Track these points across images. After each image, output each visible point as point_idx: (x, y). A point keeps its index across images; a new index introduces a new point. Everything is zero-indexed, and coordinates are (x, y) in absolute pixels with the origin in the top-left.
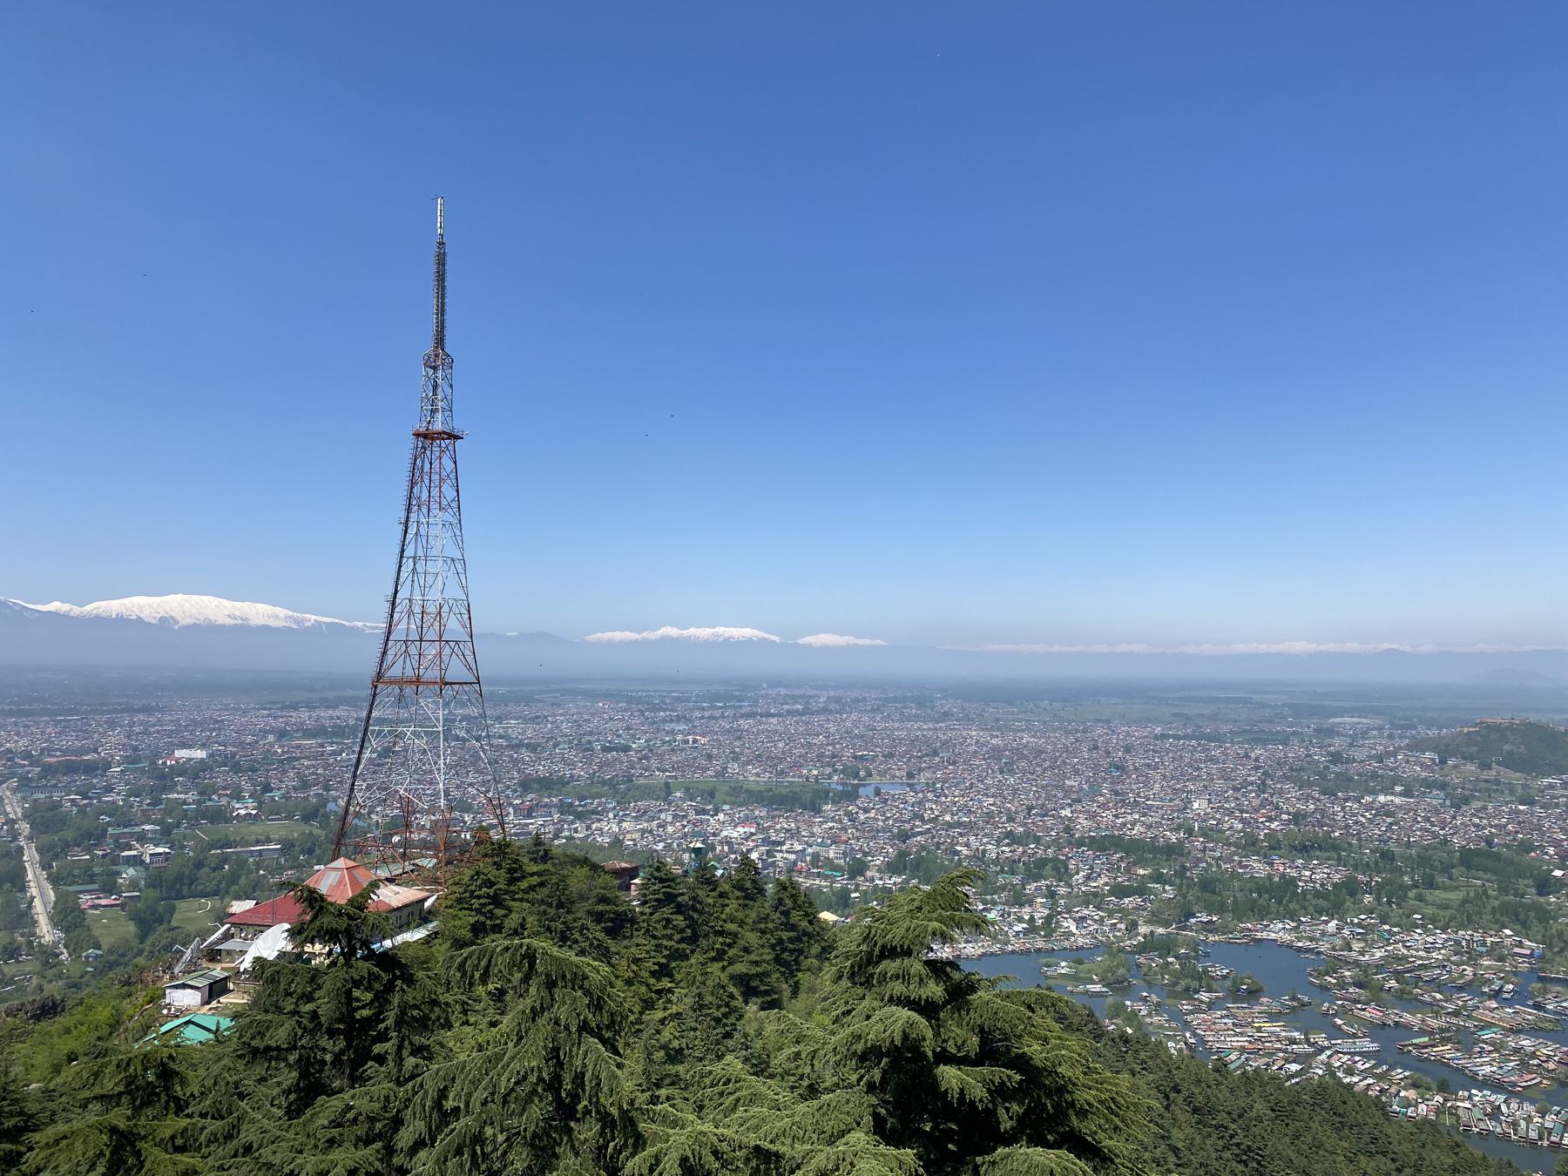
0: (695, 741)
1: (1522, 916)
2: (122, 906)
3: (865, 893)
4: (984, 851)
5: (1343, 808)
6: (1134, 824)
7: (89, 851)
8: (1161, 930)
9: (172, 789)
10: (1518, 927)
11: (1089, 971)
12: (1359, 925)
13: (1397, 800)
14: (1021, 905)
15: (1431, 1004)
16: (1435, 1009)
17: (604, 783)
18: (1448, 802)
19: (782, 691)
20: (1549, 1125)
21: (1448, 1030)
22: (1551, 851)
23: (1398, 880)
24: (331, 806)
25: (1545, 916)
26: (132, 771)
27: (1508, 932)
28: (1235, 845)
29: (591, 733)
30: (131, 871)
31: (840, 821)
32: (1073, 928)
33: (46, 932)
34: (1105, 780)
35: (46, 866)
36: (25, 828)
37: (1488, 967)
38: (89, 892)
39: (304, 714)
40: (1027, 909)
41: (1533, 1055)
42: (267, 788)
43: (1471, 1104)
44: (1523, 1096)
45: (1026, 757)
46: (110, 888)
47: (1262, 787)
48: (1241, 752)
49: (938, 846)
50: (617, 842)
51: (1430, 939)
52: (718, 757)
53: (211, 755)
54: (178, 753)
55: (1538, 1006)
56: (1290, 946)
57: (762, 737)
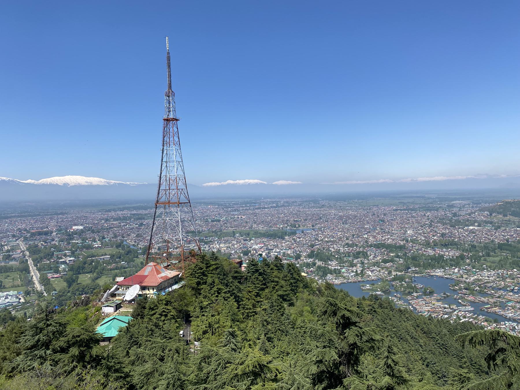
0: (241, 217)
2: (62, 277)
3: (301, 264)
4: (339, 250)
5: (458, 231)
6: (388, 239)
7: (49, 260)
8: (400, 273)
9: (73, 239)
10: (519, 268)
11: (376, 287)
12: (465, 270)
14: (353, 267)
16: (492, 296)
17: (213, 232)
18: (493, 228)
19: (269, 200)
23: (478, 254)
24: (125, 243)
26: (60, 234)
27: (515, 270)
28: (423, 245)
29: (207, 216)
30: (63, 266)
31: (291, 242)
32: (370, 274)
33: (38, 287)
34: (378, 225)
35: (36, 265)
36: (27, 253)
37: (509, 282)
38: (50, 273)
39: (113, 214)
40: (355, 268)
42: (104, 238)
45: (351, 218)
46: (57, 271)
47: (430, 226)
48: (423, 214)
49: (324, 248)
50: (219, 251)
51: (489, 273)
52: (249, 222)
53: (84, 228)
54: (74, 227)
56: (442, 277)
57: (263, 215)
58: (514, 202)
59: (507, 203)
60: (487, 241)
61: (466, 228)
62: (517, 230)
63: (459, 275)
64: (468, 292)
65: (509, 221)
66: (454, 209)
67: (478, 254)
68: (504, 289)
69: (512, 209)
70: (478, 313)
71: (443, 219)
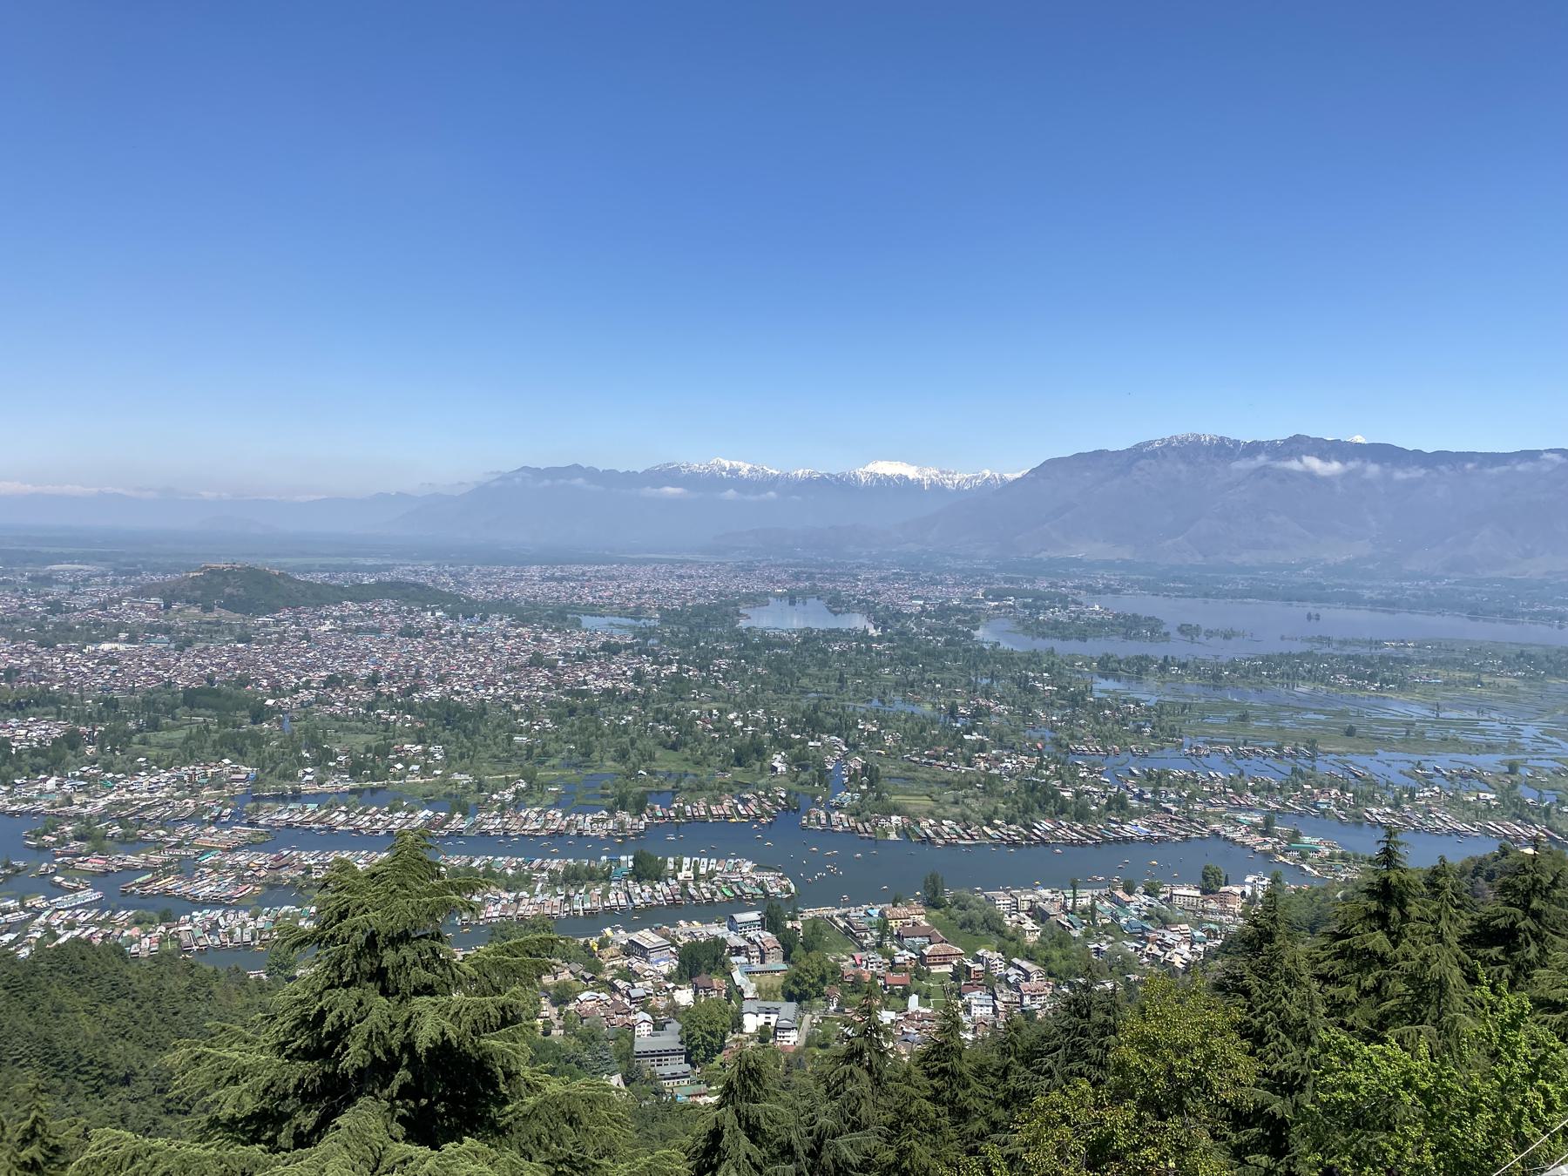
1: (239, 745)
10: (236, 756)
12: (81, 778)
13: (122, 647)
15: (154, 842)
16: (158, 845)
20: (260, 925)
21: (170, 863)
22: (265, 683)
23: (119, 727)
25: (258, 740)
27: (227, 761)
41: (248, 868)
43: (191, 927)
44: (237, 907)
51: (154, 780)
55: (252, 824)
58: (232, 572)
59: (214, 572)
60: (154, 685)
61: (91, 648)
62: (236, 650)
63: (58, 798)
64: (85, 846)
65: (218, 623)
66: (55, 589)
67: (119, 727)
68: (195, 818)
69: (228, 590)
70: (113, 905)
71: (15, 621)
